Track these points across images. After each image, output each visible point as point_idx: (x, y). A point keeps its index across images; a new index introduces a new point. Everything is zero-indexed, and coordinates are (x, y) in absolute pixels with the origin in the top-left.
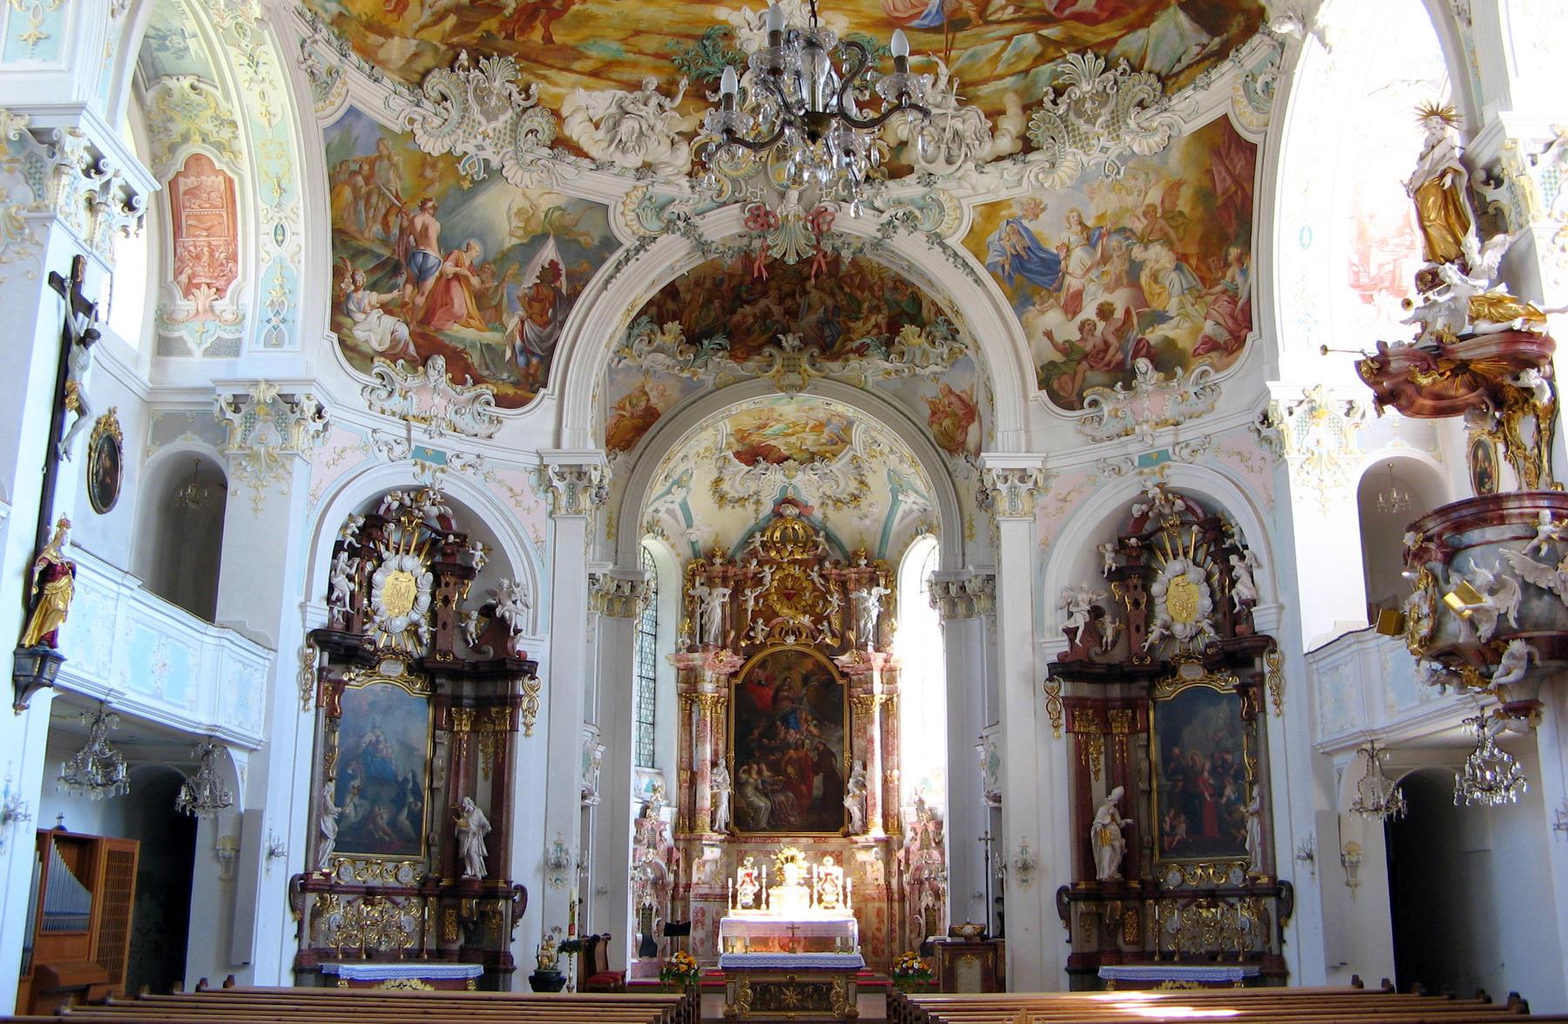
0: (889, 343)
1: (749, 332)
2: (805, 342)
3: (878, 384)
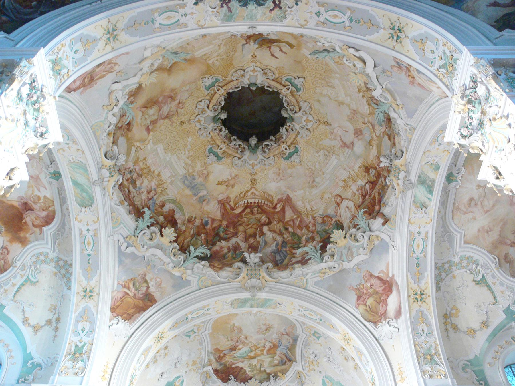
0: (323, 249)
1: (224, 257)
2: (263, 261)
3: (316, 284)
